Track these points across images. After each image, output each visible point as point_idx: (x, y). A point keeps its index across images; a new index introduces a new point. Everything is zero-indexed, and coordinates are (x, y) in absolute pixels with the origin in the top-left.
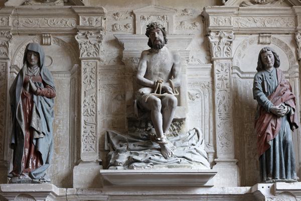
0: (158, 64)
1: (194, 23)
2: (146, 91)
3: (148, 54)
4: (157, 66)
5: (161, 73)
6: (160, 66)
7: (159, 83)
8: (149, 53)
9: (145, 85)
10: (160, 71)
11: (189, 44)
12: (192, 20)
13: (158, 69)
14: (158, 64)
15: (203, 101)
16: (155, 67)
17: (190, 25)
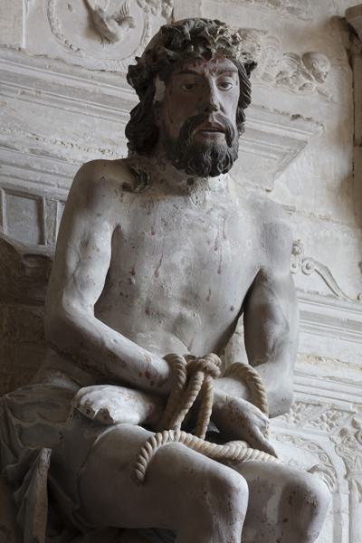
0: (181, 257)
1: (307, 57)
2: (125, 408)
3: (125, 187)
4: (172, 268)
5: (188, 313)
6: (188, 270)
7: (201, 376)
8: (127, 179)
9: (112, 370)
10: (184, 302)
11: (282, 168)
12: (293, 35)
13: (175, 285)
14: (181, 257)
15: (345, 517)
16: (166, 274)
17: (284, 64)
